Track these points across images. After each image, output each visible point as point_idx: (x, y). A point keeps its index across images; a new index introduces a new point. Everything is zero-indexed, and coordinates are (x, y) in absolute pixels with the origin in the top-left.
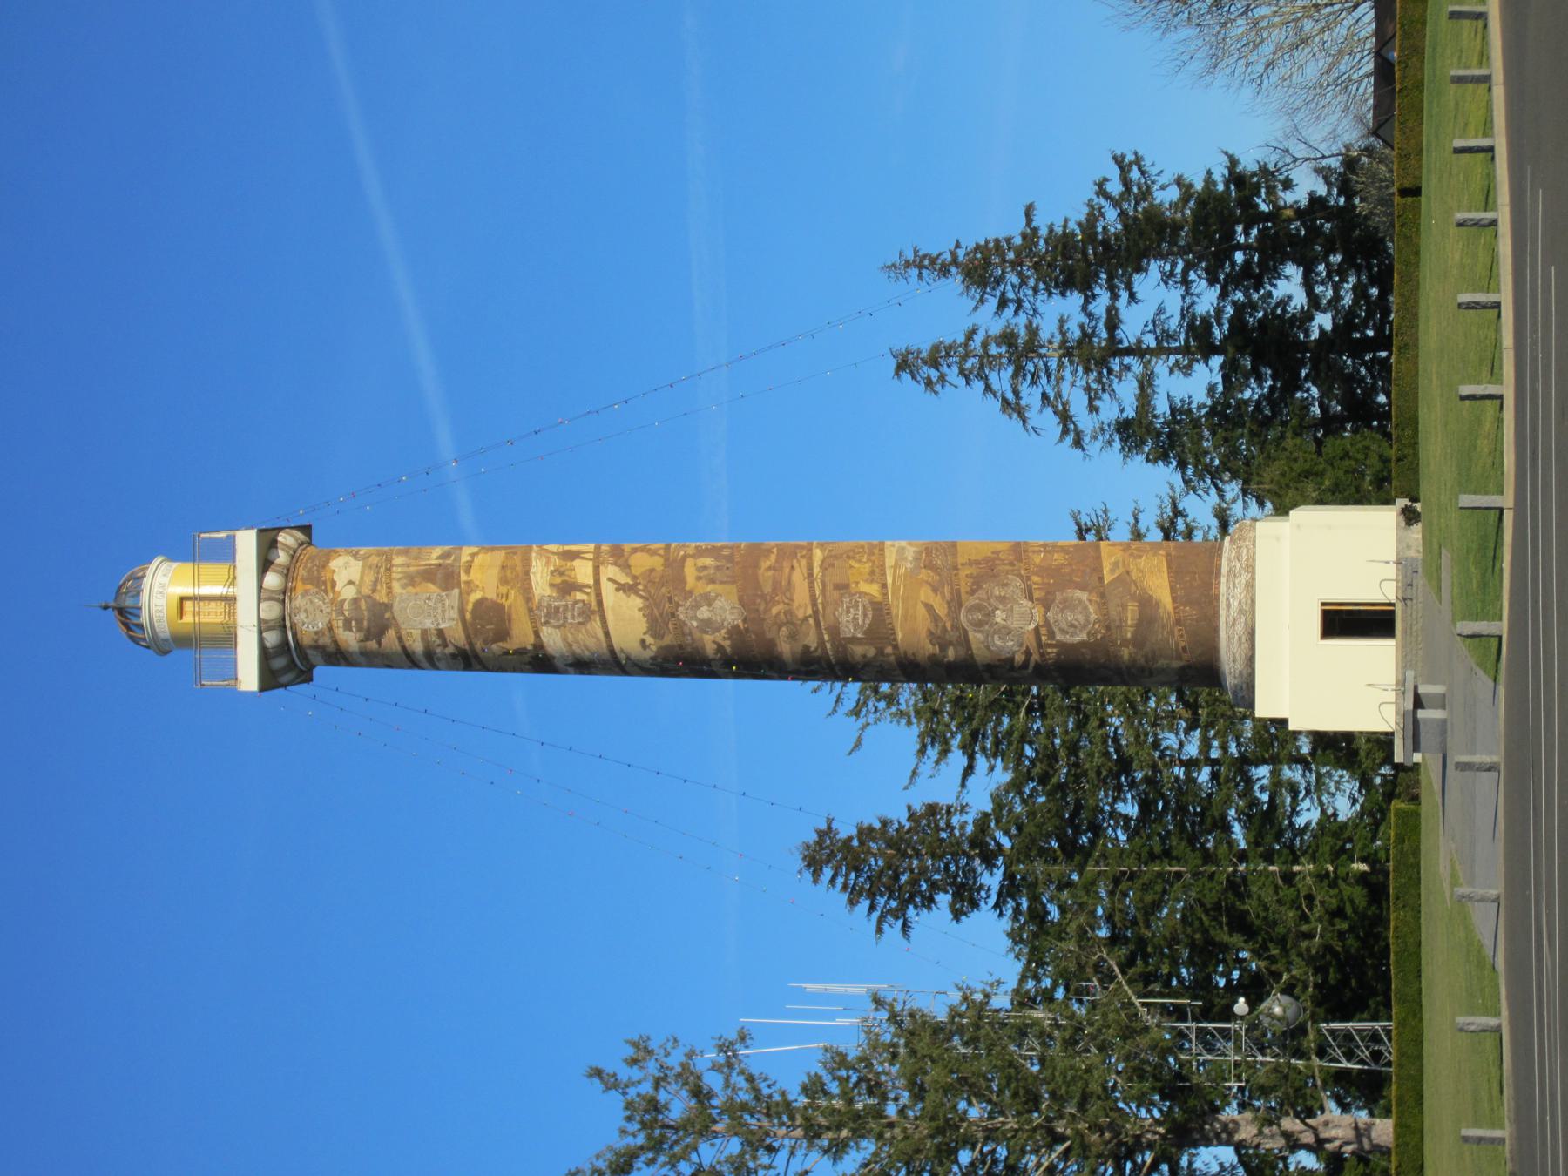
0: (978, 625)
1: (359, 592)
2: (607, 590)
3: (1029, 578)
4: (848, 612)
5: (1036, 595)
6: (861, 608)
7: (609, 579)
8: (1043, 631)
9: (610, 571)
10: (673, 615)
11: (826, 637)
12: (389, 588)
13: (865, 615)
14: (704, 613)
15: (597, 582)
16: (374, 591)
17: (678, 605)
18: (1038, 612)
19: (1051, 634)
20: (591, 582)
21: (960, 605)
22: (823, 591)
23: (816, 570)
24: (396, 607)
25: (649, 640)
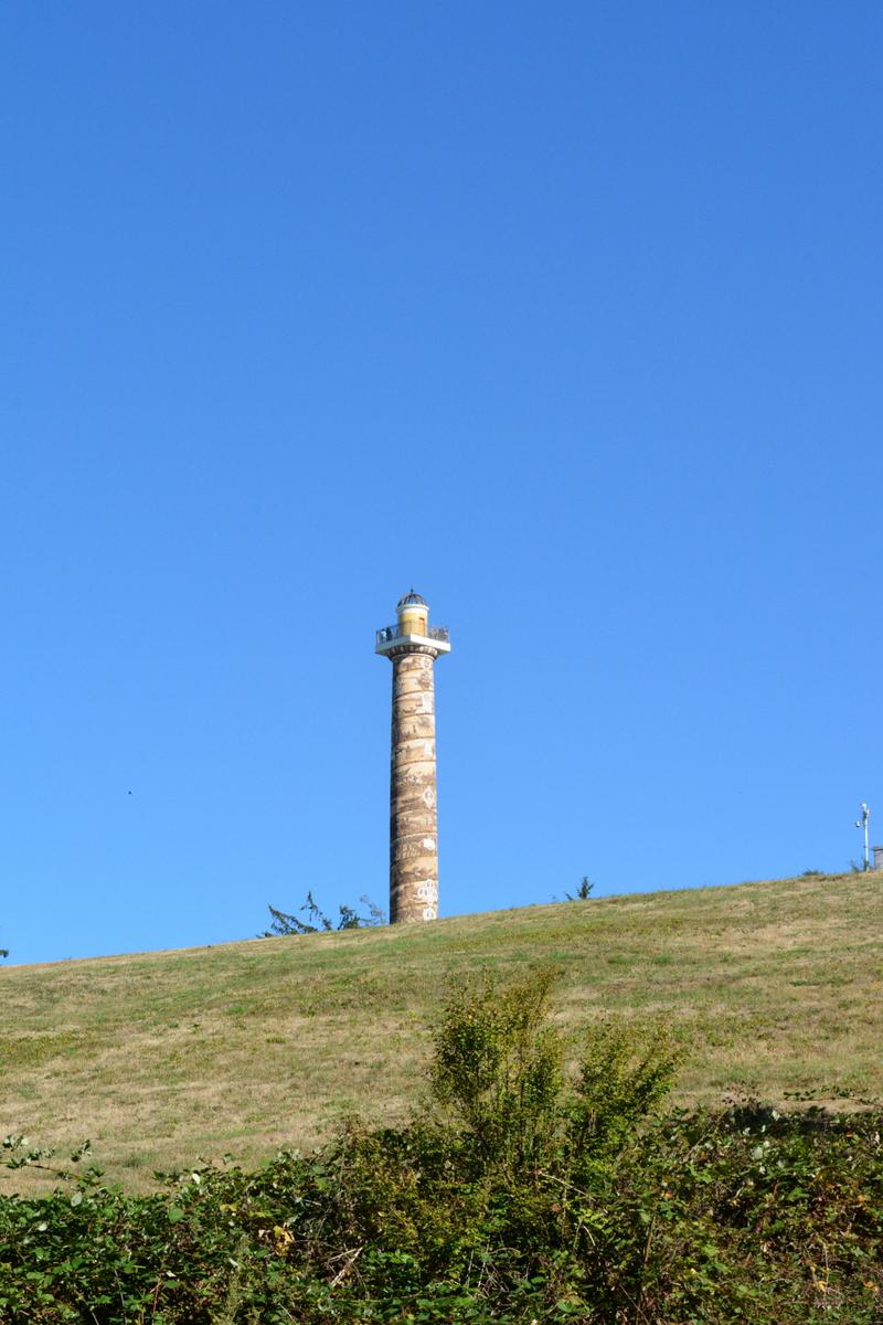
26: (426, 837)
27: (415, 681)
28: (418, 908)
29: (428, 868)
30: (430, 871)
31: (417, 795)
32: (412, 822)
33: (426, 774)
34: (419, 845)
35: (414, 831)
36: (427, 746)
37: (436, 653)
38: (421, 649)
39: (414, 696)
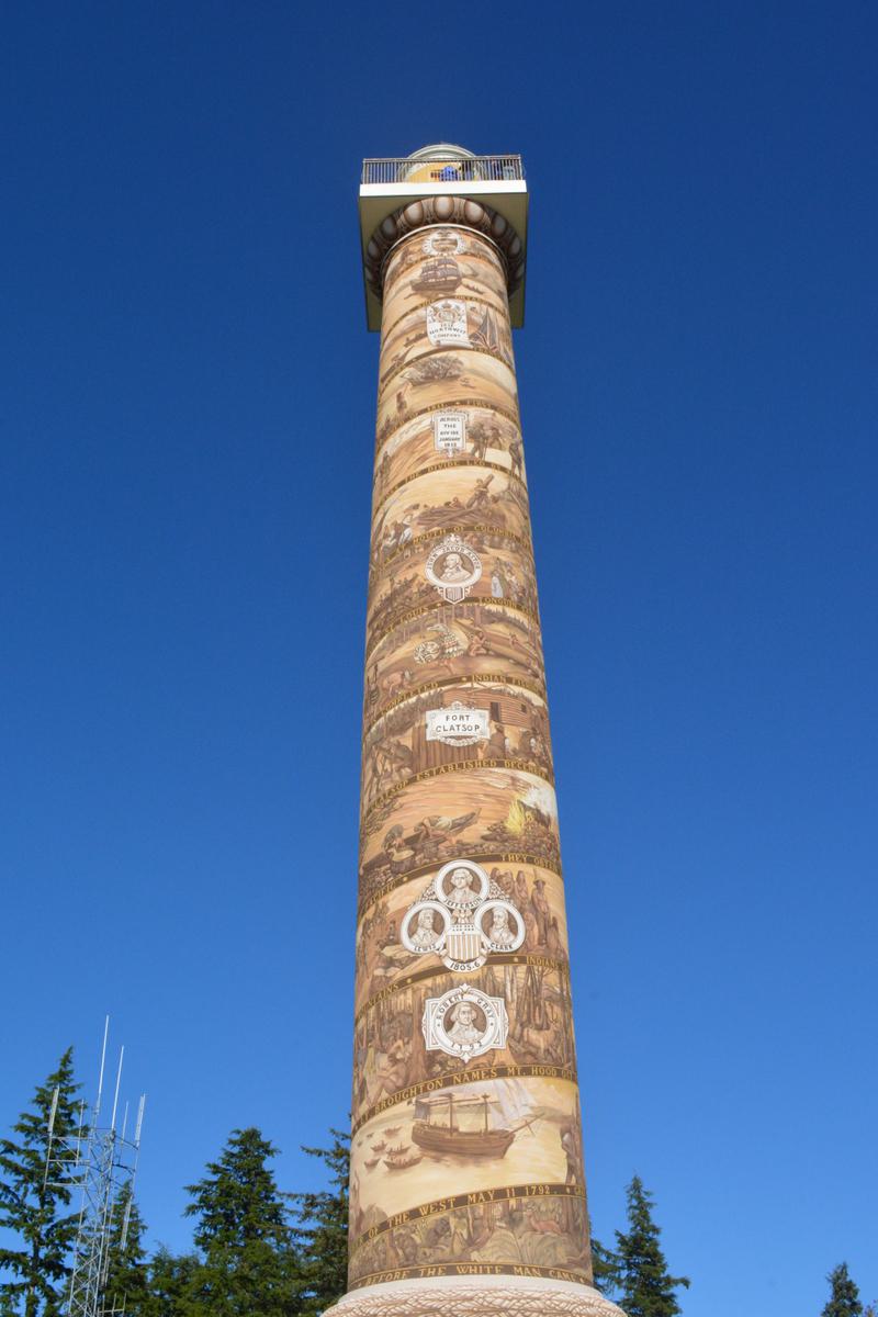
0: (449, 887)
1: (465, 276)
2: (482, 473)
3: (522, 960)
4: (462, 717)
5: (499, 970)
6: (467, 733)
7: (491, 478)
8: (440, 980)
9: (499, 484)
10: (450, 531)
11: (423, 695)
12: (471, 299)
13: (459, 738)
14: (453, 559)
15: (488, 465)
16: (468, 287)
17: (463, 537)
18: (474, 970)
19: (436, 992)
20: (488, 458)
21: (477, 860)
22: (489, 690)
23: (515, 689)
24: (450, 302)
25: (417, 513)
26: (438, 703)
27: (409, 290)
28: (404, 1000)
29: (446, 821)
30: (460, 825)
31: (404, 575)
32: (387, 672)
33: (438, 503)
34: (407, 740)
35: (394, 698)
36: (441, 427)
37: (475, 210)
38: (413, 211)
39: (403, 325)
